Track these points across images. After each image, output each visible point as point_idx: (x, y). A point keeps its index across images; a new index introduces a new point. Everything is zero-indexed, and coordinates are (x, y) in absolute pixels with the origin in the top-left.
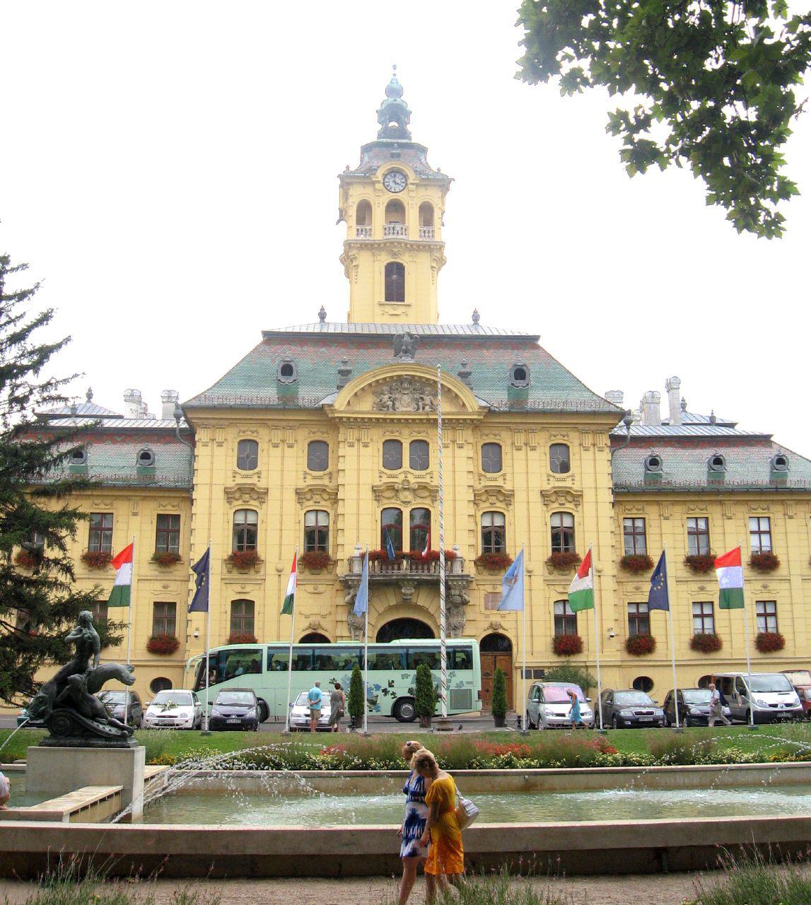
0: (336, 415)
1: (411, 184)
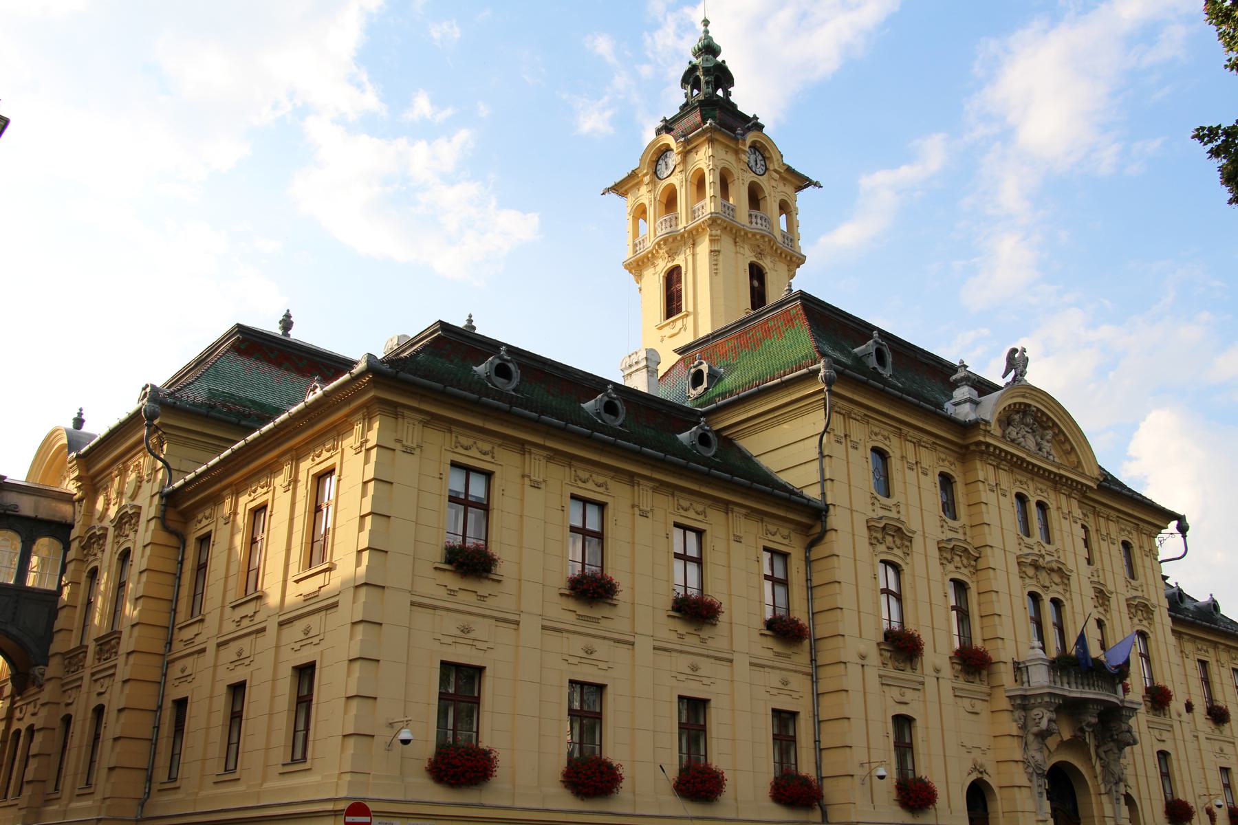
0: (989, 440)
1: (776, 171)
